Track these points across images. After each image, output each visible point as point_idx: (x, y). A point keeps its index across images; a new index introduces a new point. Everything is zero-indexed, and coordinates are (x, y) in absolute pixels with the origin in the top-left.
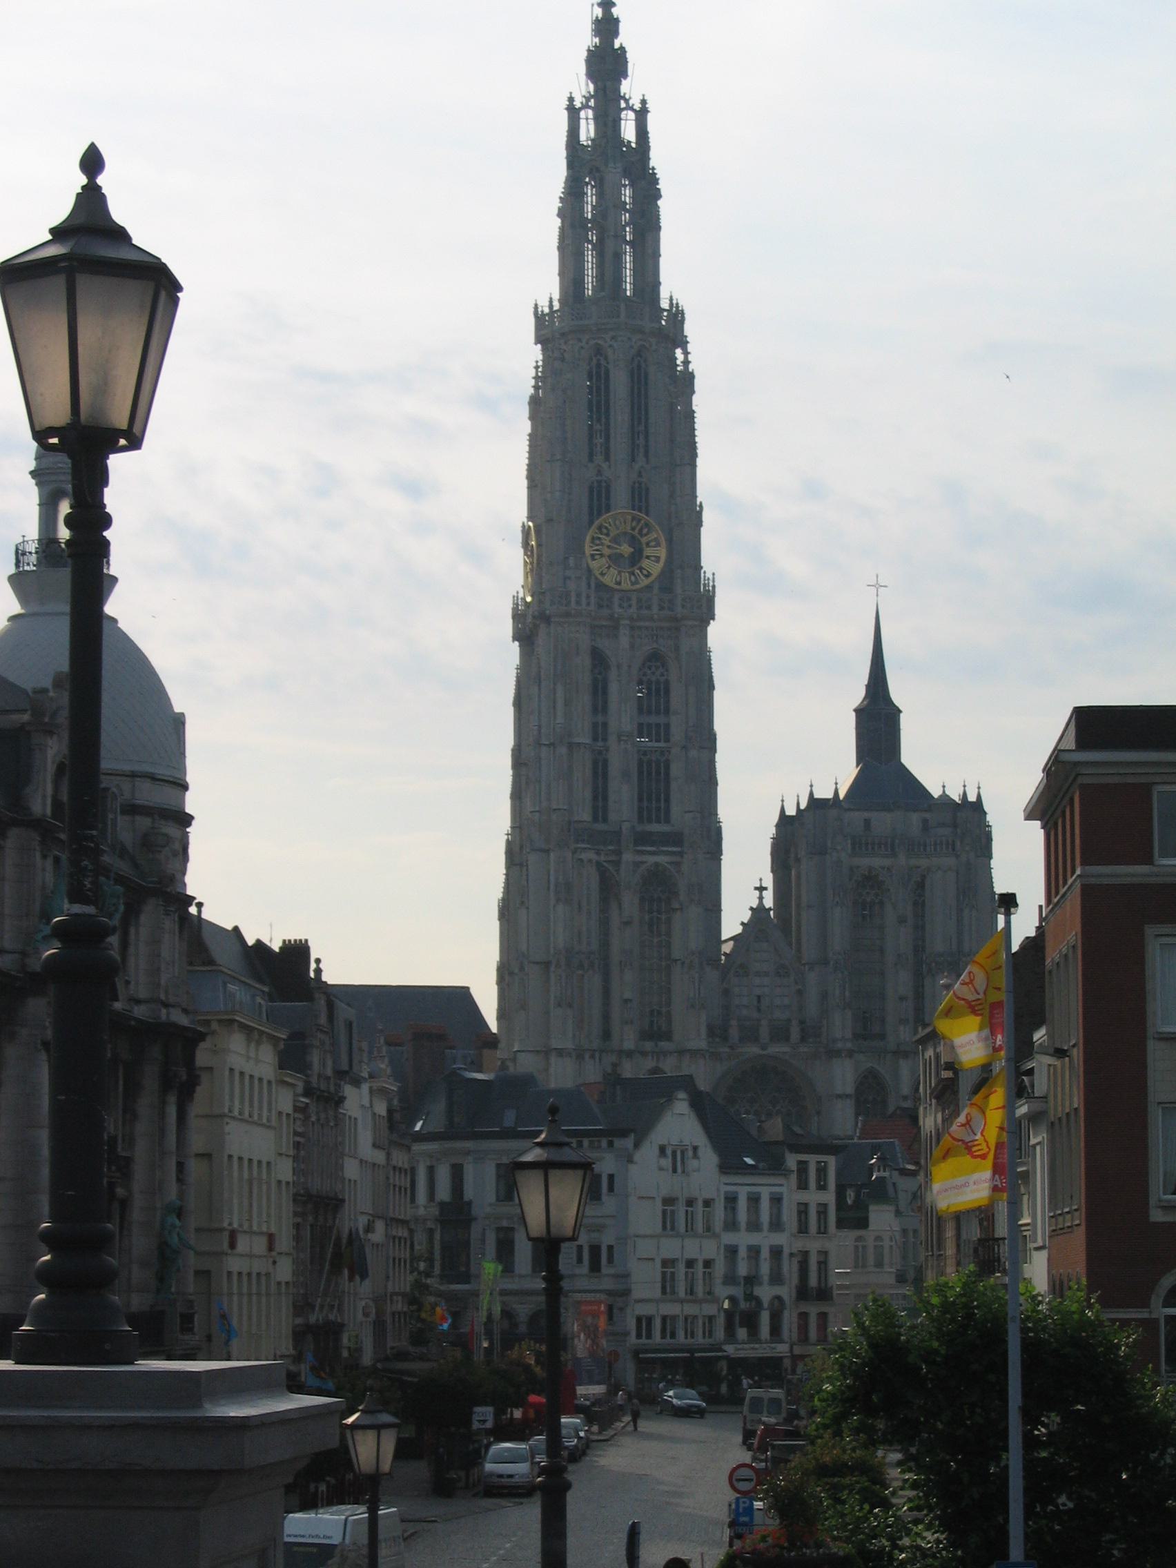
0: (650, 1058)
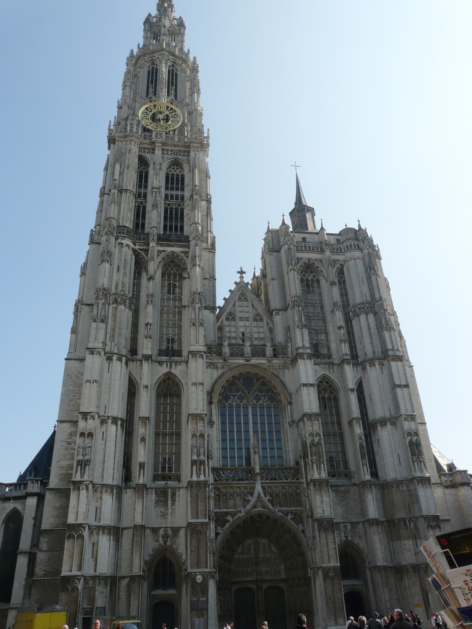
0: (165, 365)
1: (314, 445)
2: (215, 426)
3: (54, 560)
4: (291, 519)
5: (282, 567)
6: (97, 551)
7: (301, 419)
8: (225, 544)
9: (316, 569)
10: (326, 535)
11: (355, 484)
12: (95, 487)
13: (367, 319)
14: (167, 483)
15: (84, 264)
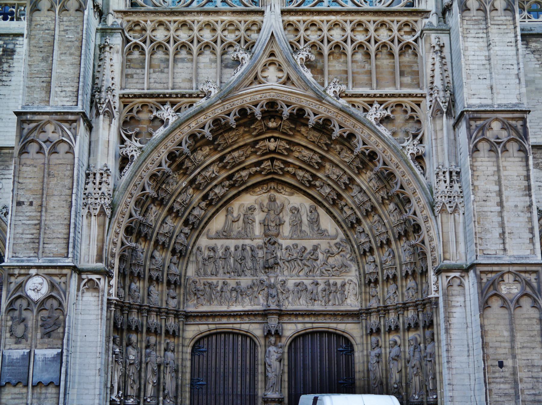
9: (458, 274)
10: (498, 167)
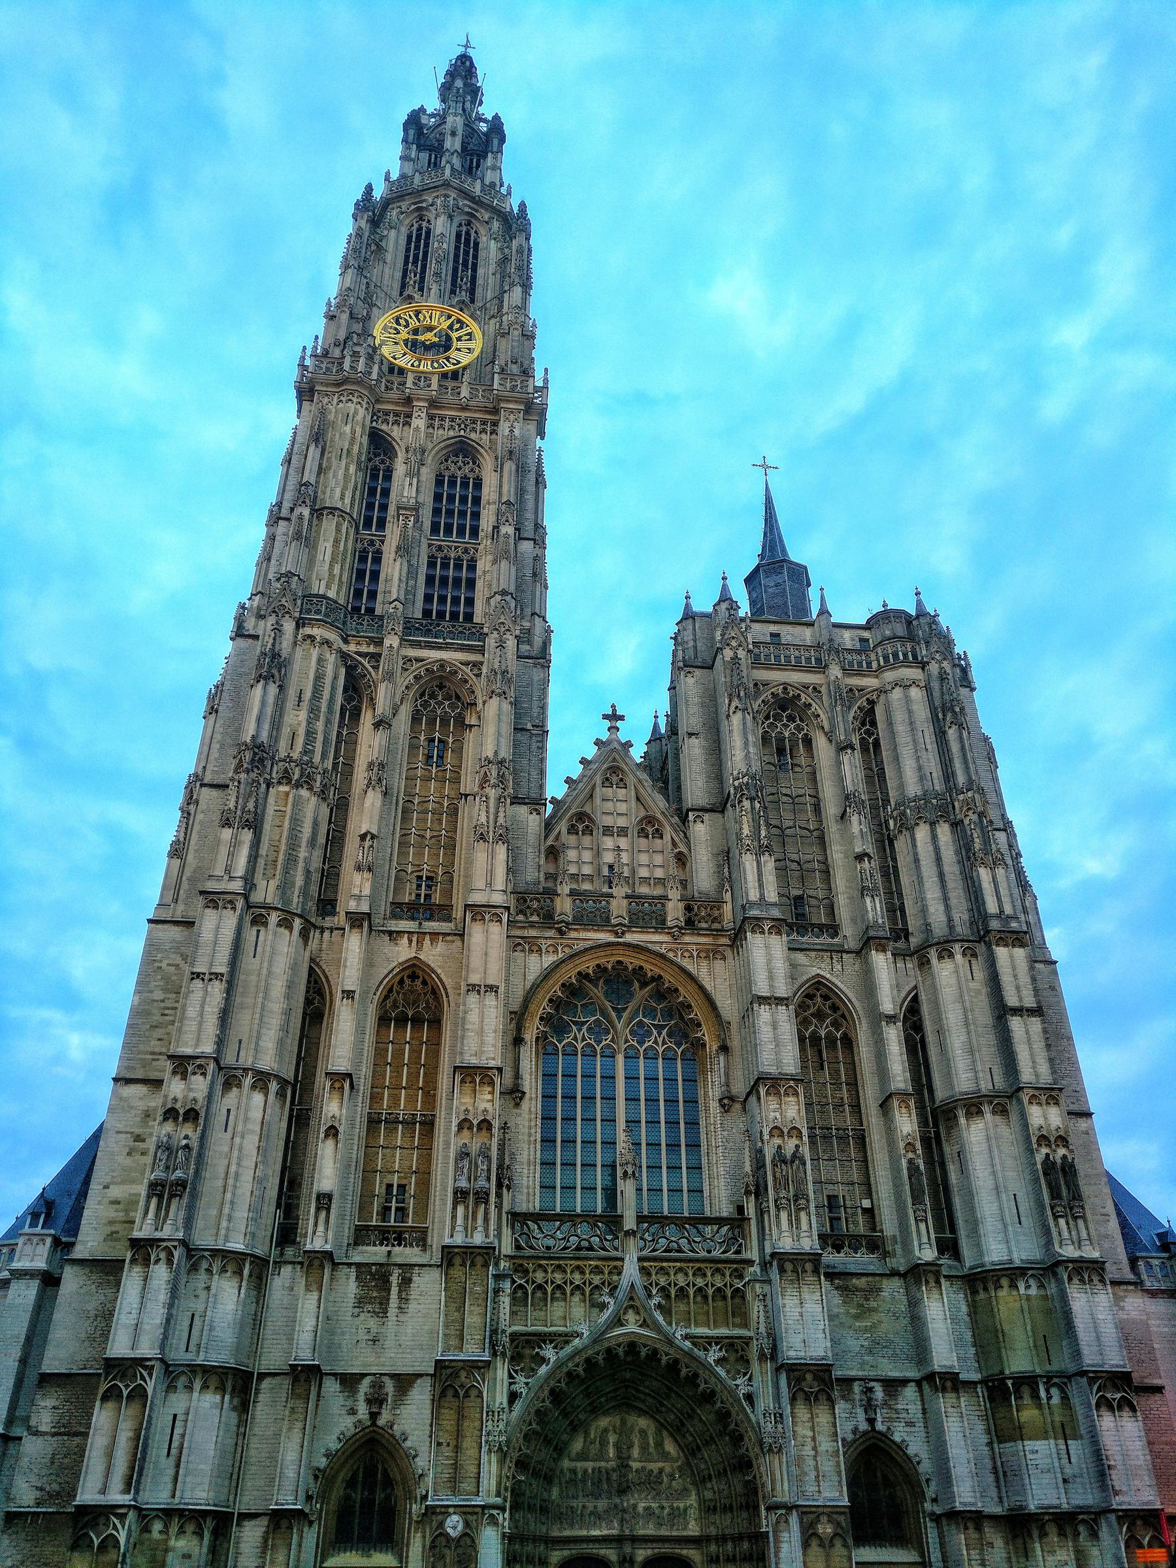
1: (784, 1162)
2: (525, 1104)
3: (66, 1461)
4: (719, 1362)
5: (692, 1500)
6: (183, 1436)
7: (753, 1090)
8: (534, 1426)
9: (783, 1512)
11: (894, 1273)
12: (194, 1256)
13: (934, 837)
14: (389, 1252)
15: (217, 687)
